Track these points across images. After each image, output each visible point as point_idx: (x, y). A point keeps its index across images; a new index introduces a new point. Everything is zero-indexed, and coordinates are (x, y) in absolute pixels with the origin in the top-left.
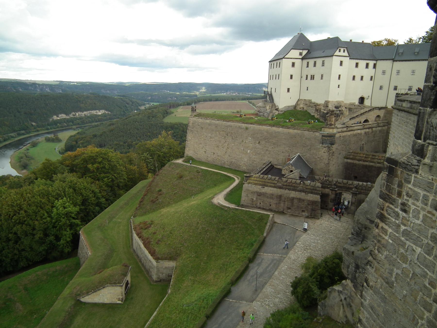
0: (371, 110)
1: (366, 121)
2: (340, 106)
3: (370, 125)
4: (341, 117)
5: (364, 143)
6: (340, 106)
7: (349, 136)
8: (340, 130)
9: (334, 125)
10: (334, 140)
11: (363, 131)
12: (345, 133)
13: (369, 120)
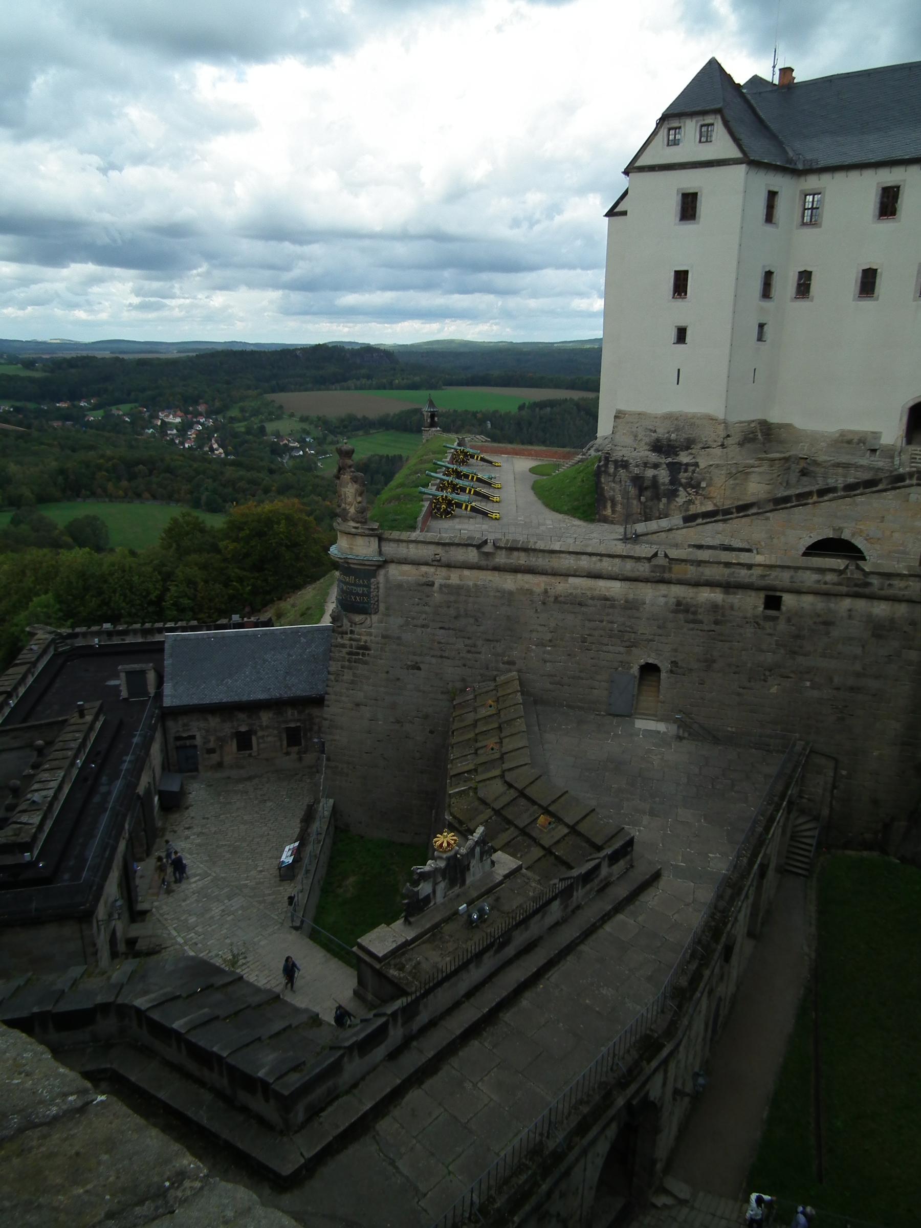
2: (688, 445)
3: (744, 572)
5: (665, 666)
6: (688, 445)
7: (508, 597)
9: (353, 520)
10: (360, 590)
11: (650, 594)
12: (467, 573)
13: (859, 542)
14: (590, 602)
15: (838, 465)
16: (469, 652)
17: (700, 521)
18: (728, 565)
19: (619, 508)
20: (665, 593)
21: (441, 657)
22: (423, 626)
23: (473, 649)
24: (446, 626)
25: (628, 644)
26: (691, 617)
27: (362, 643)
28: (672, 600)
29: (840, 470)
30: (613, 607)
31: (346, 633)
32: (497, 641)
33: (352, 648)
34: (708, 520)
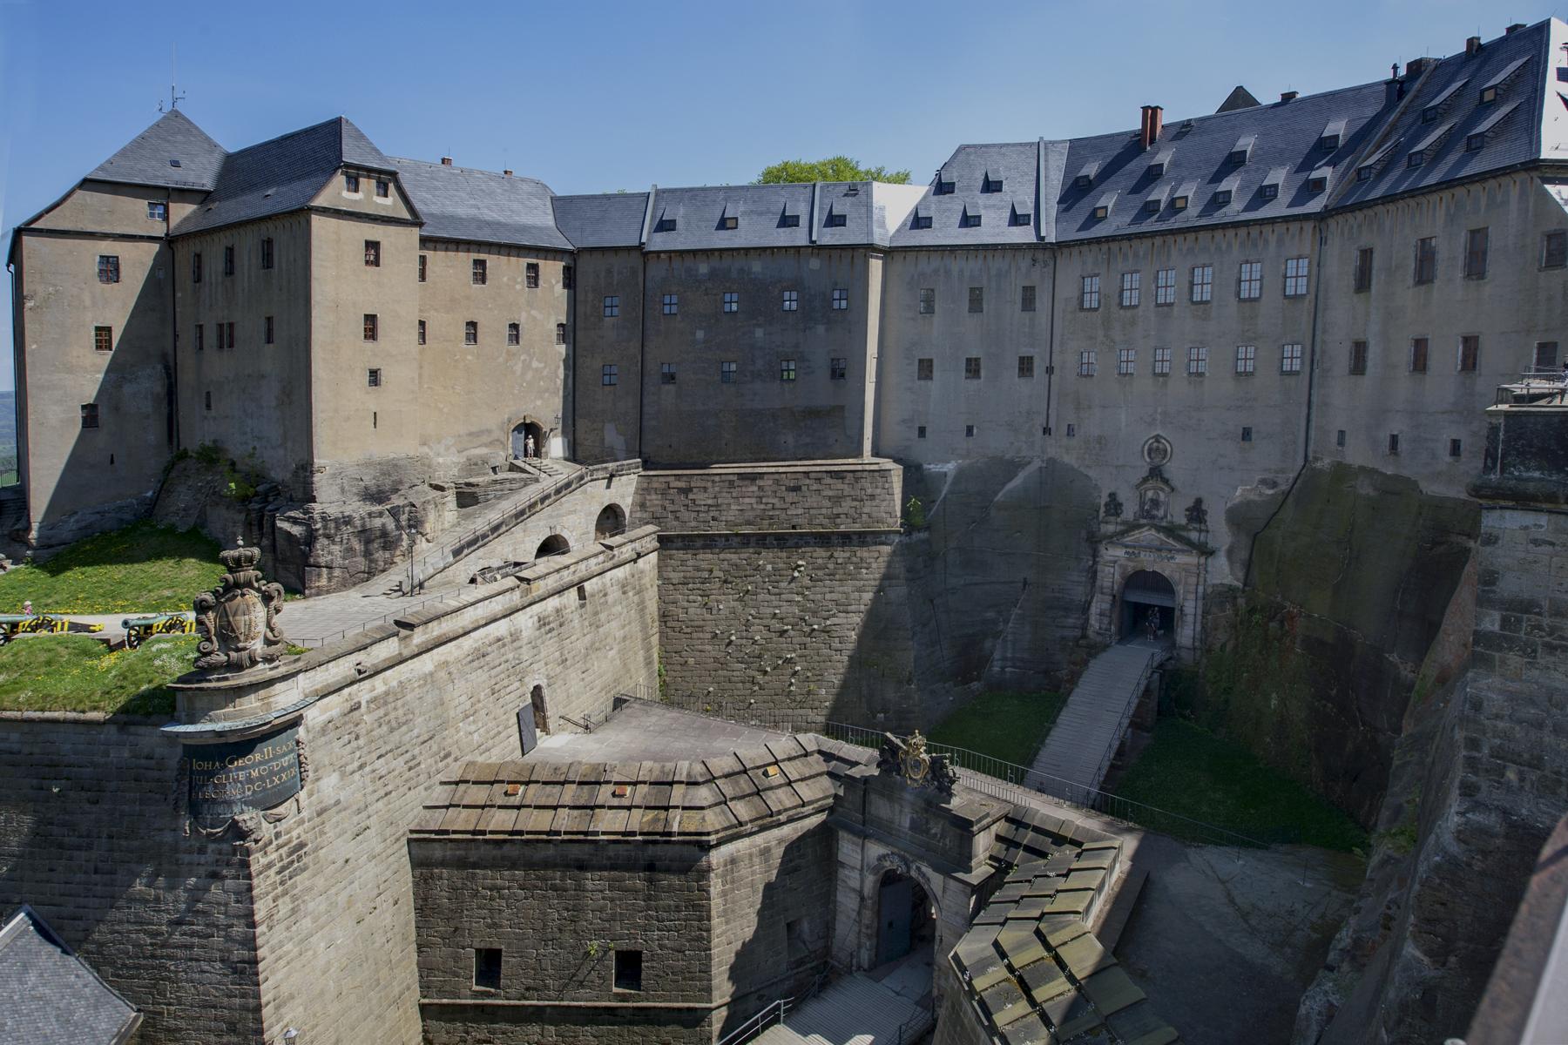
0: (568, 485)
1: (552, 546)
3: (565, 573)
4: (405, 543)
8: (342, 669)
11: (525, 621)
13: (565, 534)
14: (489, 649)
15: (495, 482)
16: (410, 769)
17: (466, 551)
18: (558, 571)
19: (337, 572)
20: (530, 613)
21: (386, 794)
22: (361, 767)
23: (412, 764)
24: (383, 751)
25: (519, 677)
26: (547, 628)
27: (295, 842)
28: (536, 618)
29: (498, 487)
30: (504, 645)
31: (271, 842)
32: (431, 738)
33: (282, 860)
34: (472, 548)
